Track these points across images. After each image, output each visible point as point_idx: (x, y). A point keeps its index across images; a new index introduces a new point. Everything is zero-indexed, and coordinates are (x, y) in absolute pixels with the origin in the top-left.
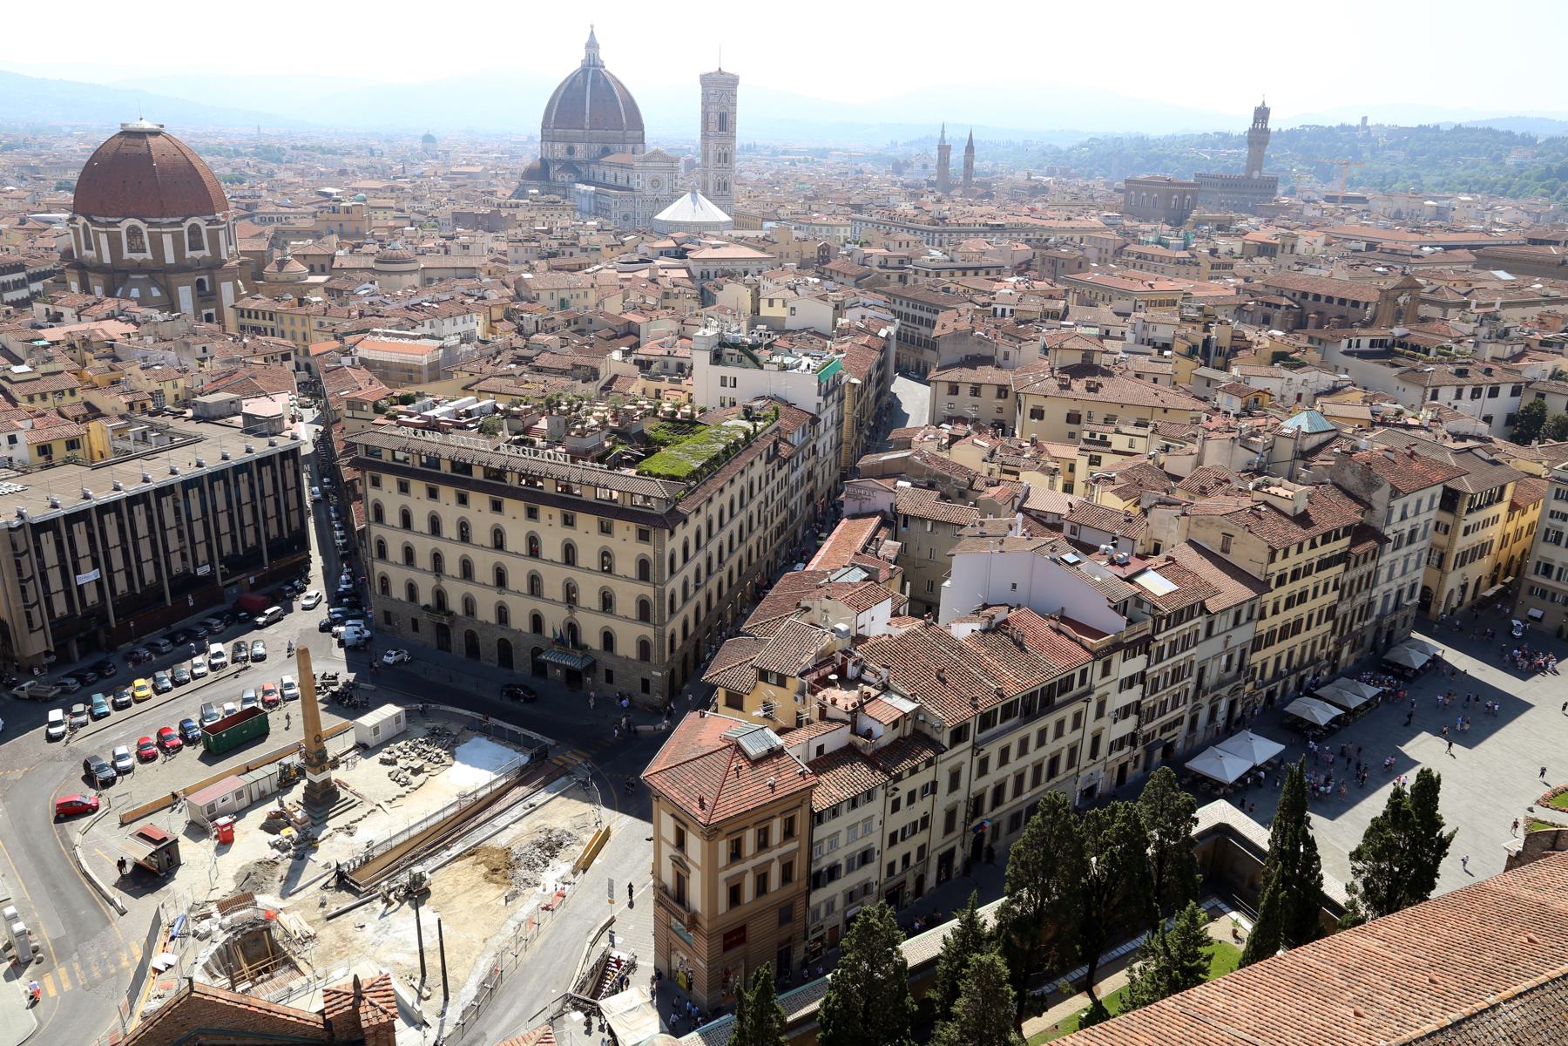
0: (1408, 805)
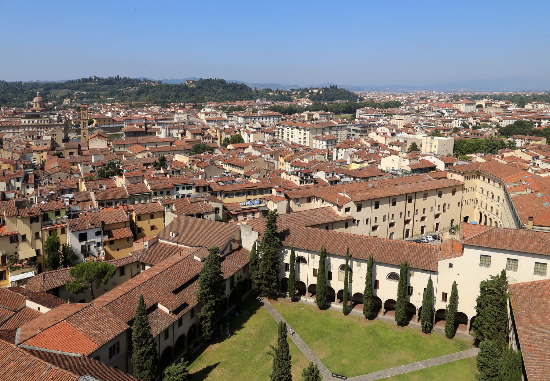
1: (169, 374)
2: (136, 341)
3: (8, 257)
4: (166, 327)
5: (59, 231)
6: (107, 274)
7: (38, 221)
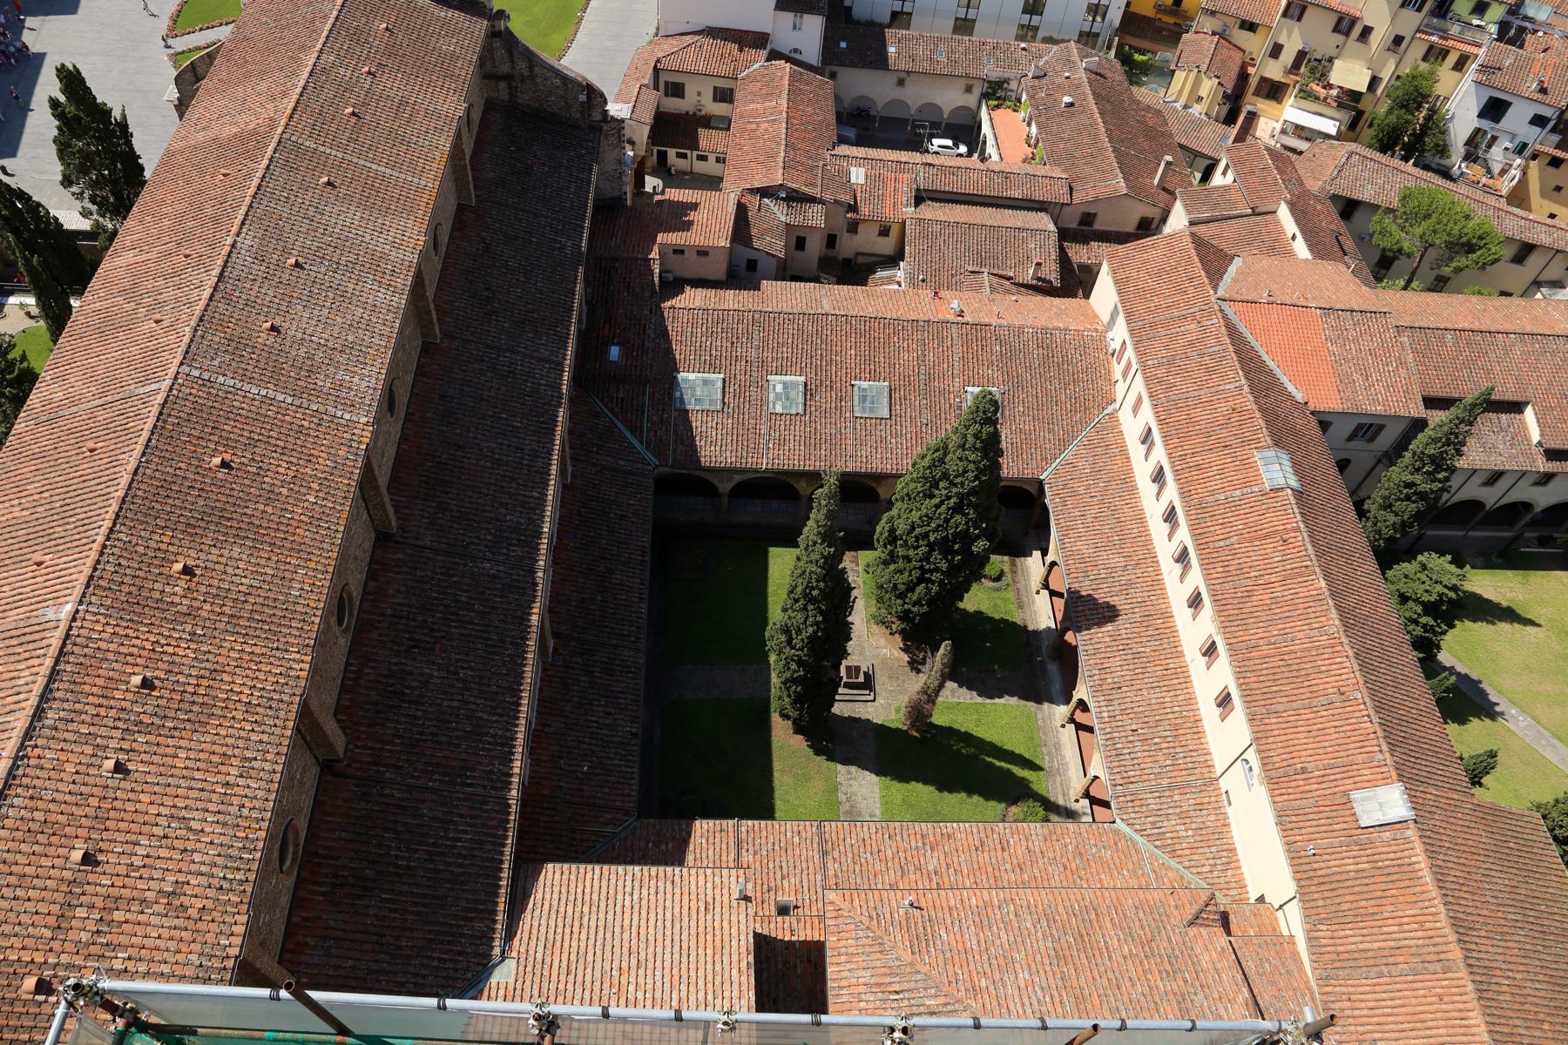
1: (1424, 567)
2: (1414, 453)
3: (1309, 61)
5: (1452, 58)
6: (1474, 256)
7: (1419, 10)
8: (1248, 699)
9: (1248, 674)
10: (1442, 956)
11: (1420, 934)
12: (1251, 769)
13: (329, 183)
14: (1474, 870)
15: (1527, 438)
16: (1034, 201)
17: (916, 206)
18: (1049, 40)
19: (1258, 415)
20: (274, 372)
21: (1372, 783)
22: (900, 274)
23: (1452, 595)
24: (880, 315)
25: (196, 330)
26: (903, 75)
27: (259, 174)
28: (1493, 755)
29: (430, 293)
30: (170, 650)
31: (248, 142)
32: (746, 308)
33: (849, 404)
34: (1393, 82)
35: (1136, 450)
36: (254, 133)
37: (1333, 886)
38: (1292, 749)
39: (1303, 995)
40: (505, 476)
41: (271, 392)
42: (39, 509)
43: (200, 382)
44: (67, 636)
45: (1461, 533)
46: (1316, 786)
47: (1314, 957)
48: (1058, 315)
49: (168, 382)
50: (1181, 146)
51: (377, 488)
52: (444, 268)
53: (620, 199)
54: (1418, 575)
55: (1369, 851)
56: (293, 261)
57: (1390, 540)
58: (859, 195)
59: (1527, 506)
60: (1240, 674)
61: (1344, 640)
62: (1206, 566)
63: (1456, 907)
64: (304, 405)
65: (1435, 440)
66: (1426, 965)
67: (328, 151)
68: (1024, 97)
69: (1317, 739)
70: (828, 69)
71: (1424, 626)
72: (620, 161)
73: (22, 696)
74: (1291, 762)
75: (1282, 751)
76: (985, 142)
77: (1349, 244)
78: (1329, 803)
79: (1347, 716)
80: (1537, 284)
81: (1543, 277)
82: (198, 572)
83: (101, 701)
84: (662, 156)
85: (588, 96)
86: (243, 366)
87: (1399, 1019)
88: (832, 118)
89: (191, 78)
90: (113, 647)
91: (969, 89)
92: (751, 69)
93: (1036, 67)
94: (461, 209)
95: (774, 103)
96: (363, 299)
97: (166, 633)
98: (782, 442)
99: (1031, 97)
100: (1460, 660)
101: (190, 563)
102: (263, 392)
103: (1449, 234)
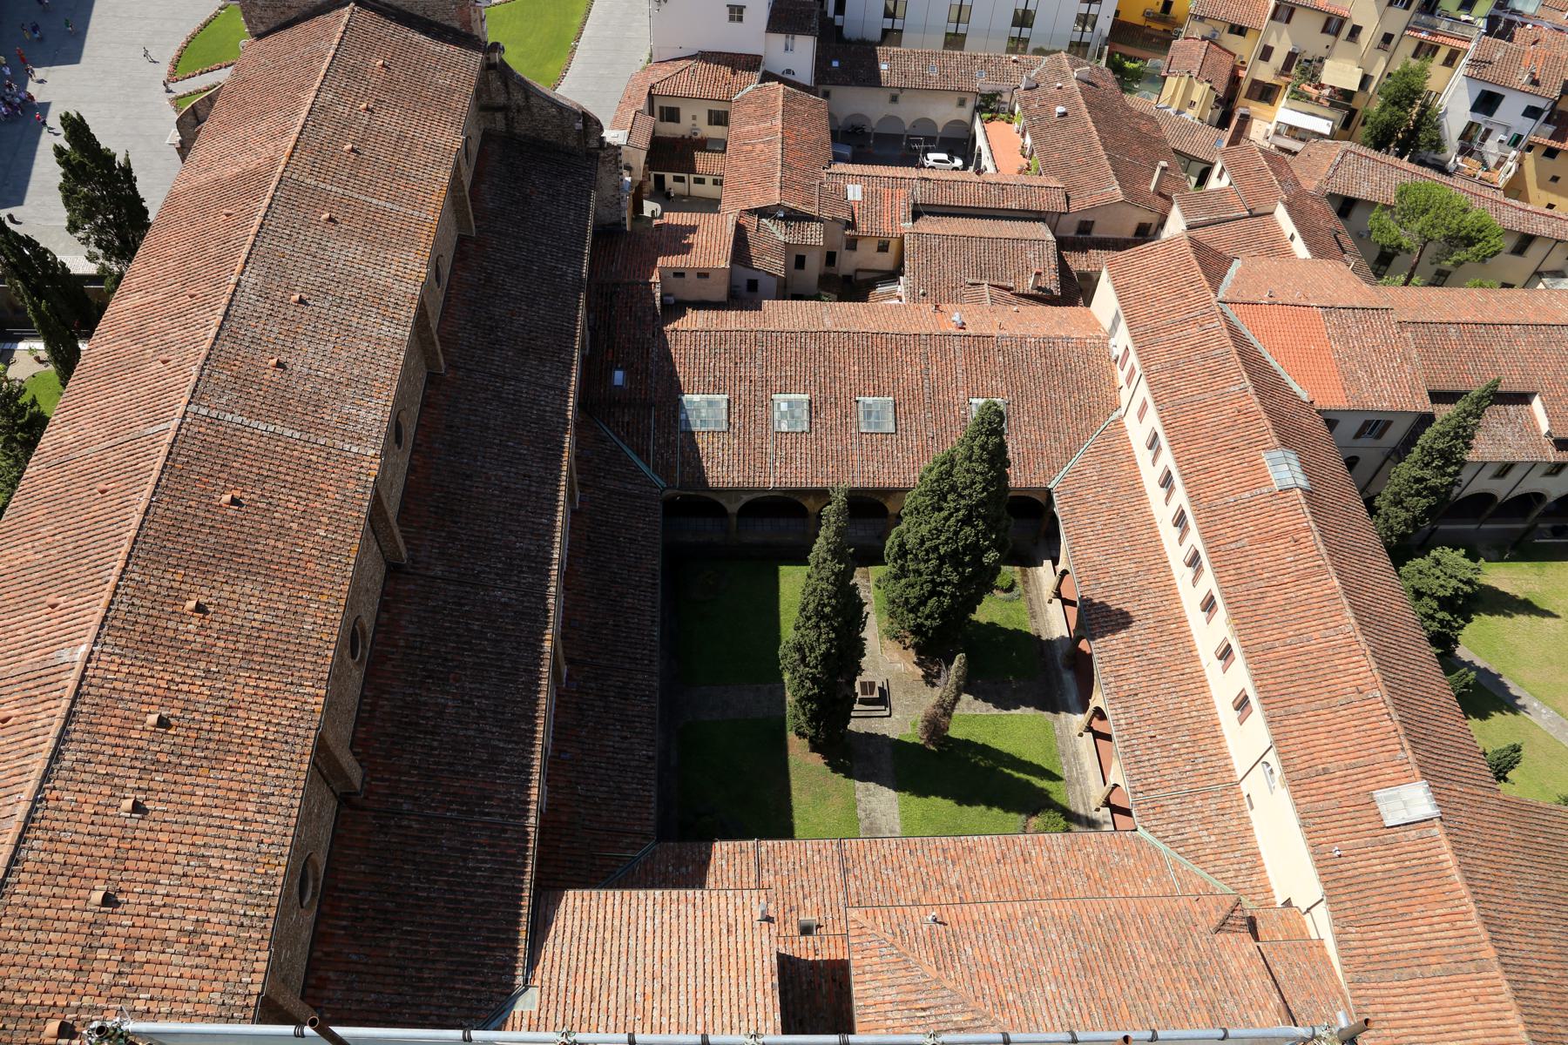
0: (76, 157)
1: (1438, 562)
2: (1423, 448)
3: (1300, 62)
4: (1512, 460)
5: (1443, 54)
7: (1407, 7)
8: (1266, 701)
9: (1265, 676)
10: (1476, 955)
11: (1451, 933)
12: (1271, 771)
13: (330, 219)
14: (1503, 866)
15: (1536, 429)
16: (1031, 211)
17: (914, 221)
18: (1040, 52)
19: (1264, 416)
20: (281, 408)
21: (1396, 782)
22: (900, 290)
23: (1467, 589)
24: (882, 331)
25: (203, 369)
26: (896, 92)
27: (261, 213)
28: (1516, 749)
29: (434, 324)
30: (185, 688)
31: (250, 182)
32: (748, 328)
33: (855, 420)
34: (1384, 79)
35: (1143, 455)
36: (255, 172)
37: (1361, 887)
38: (1312, 750)
39: (1335, 1000)
40: (512, 504)
41: (278, 428)
42: (52, 552)
43: (208, 420)
44: (83, 677)
45: (1474, 527)
46: (1338, 787)
47: (1344, 960)
48: (1059, 324)
49: (177, 422)
50: (1176, 151)
51: (387, 520)
52: (447, 299)
53: (619, 225)
54: (1433, 570)
55: (1395, 851)
56: (296, 297)
57: (1403, 536)
58: (856, 211)
59: (1539, 497)
60: (1256, 677)
61: (1361, 638)
62: (1218, 569)
63: (1487, 905)
64: (312, 440)
65: (1443, 435)
66: (1460, 965)
67: (329, 188)
68: (1017, 108)
69: (1338, 739)
70: (822, 88)
71: (1441, 621)
72: (618, 187)
73: (39, 739)
74: (1312, 763)
75: (1302, 752)
76: (980, 155)
77: (1348, 242)
78: (1352, 803)
79: (1367, 714)
80: (1538, 274)
81: (1544, 268)
82: (211, 609)
83: (118, 741)
84: (660, 181)
85: (585, 125)
86: (251, 403)
87: (1434, 1021)
88: (827, 137)
89: (192, 121)
90: (128, 686)
91: (962, 103)
92: (745, 92)
93: (1028, 78)
94: (462, 240)
95: (769, 124)
96: (368, 333)
97: (181, 671)
98: (788, 460)
99: (1024, 109)
100: (1479, 655)
101: (203, 600)
102: (271, 428)
103: (1448, 229)
